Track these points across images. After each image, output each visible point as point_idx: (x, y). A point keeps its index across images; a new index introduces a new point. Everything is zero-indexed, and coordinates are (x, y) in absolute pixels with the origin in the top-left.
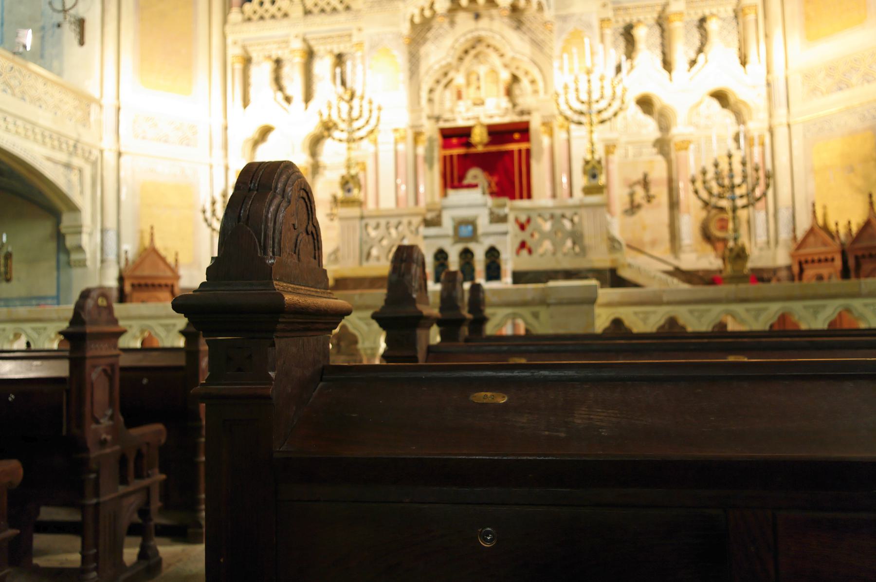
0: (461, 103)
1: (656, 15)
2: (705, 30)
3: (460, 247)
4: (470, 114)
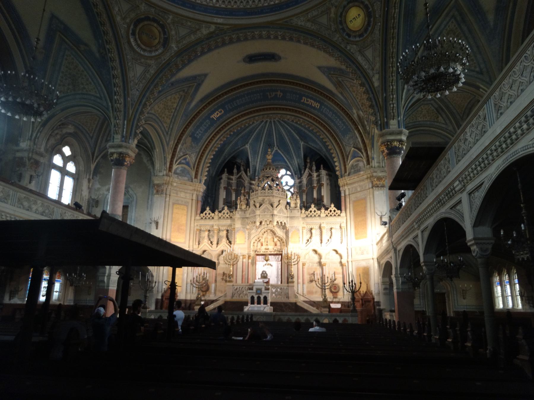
1: (318, 226)
3: (257, 296)
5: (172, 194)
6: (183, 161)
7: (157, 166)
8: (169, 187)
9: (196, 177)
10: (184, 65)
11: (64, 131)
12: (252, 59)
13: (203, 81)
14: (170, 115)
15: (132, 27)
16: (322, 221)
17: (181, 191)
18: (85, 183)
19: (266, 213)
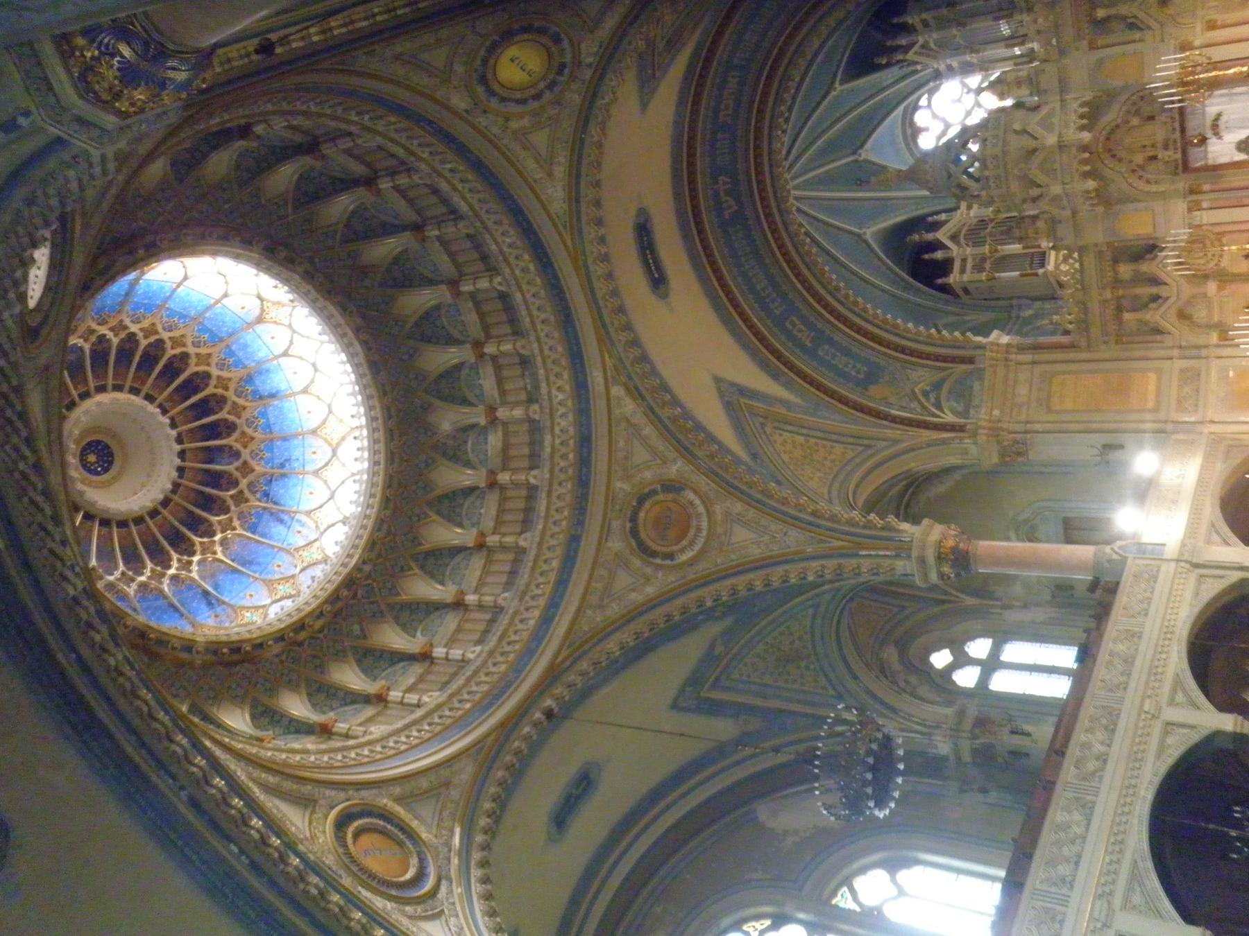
0: (1160, 156)
5: (1023, 417)
6: (933, 400)
7: (954, 460)
8: (1005, 426)
9: (971, 360)
10: (711, 438)
11: (897, 666)
12: (658, 281)
13: (733, 384)
14: (824, 446)
15: (658, 561)
17: (1014, 394)
18: (1013, 616)
19: (1057, 166)
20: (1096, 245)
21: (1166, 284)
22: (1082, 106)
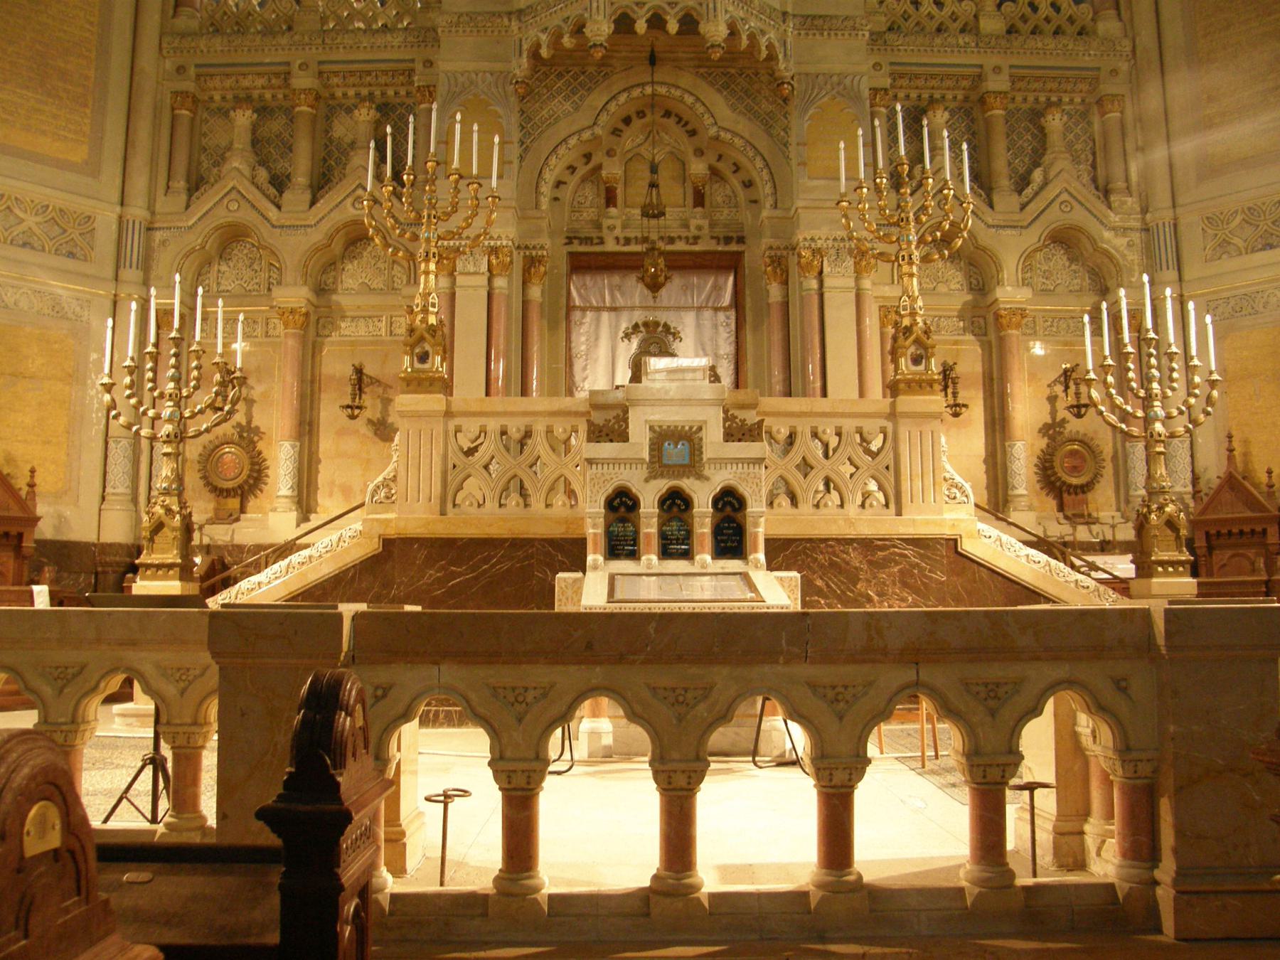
0: (613, 211)
2: (1042, 129)
4: (631, 234)
16: (990, 61)
20: (429, 63)
21: (313, 203)
22: (770, 46)
